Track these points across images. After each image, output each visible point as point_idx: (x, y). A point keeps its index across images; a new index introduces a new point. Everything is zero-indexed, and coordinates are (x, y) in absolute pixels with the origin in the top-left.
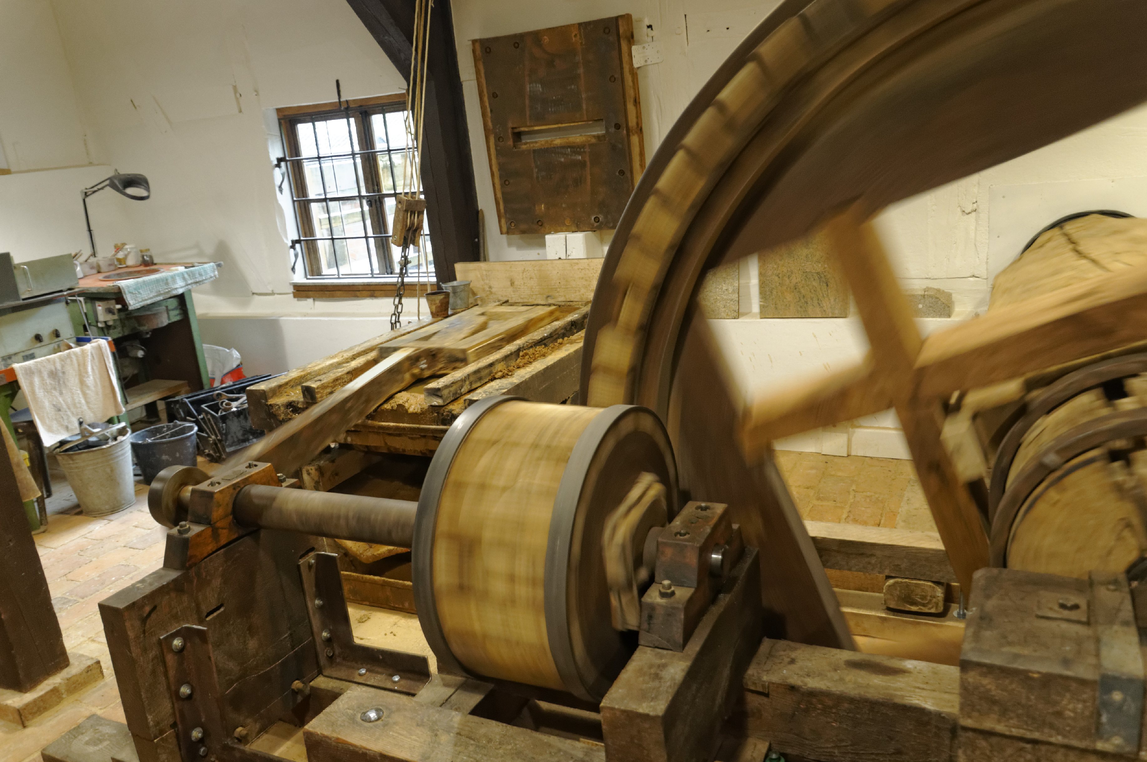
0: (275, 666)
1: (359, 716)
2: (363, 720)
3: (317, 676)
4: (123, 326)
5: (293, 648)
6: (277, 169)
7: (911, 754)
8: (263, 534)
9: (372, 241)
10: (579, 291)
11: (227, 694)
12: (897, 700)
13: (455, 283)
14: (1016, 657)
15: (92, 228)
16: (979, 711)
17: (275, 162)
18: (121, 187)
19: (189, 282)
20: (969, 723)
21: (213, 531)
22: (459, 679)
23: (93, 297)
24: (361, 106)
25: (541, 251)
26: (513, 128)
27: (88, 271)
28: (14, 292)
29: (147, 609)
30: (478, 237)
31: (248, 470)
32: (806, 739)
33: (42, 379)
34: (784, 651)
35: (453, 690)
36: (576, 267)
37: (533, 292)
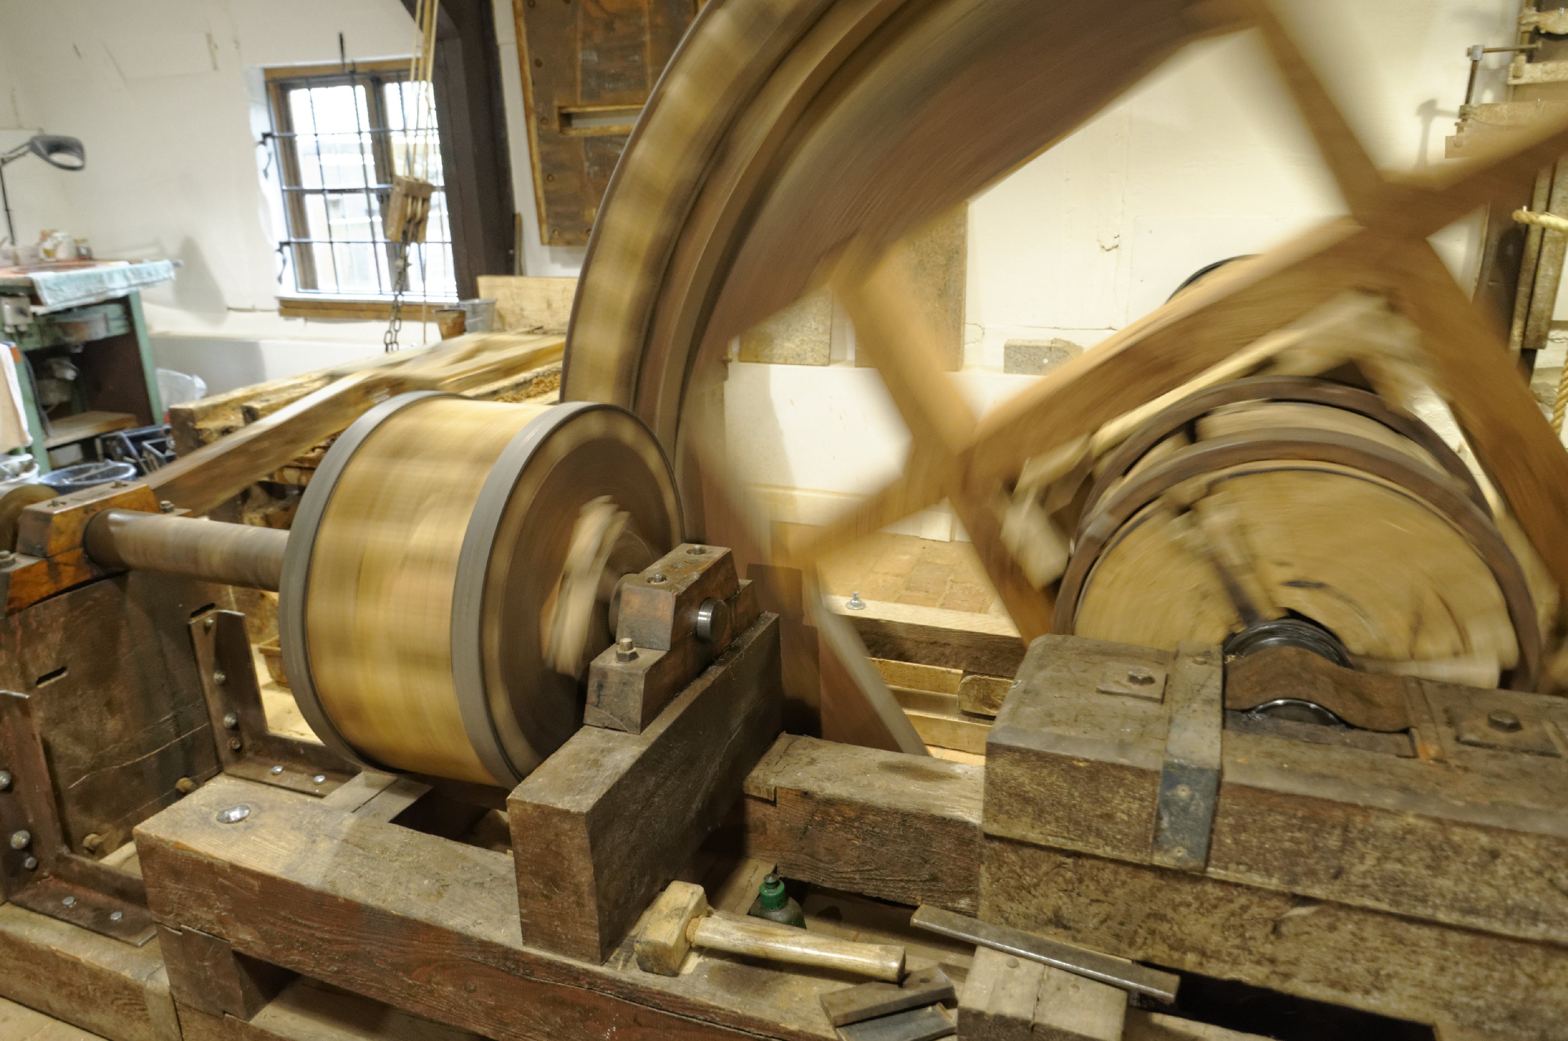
0: (149, 757)
1: (216, 814)
2: (219, 820)
3: (216, 775)
4: (42, 333)
5: (178, 735)
6: (262, 147)
7: (950, 880)
8: (132, 578)
9: (382, 249)
11: (72, 789)
12: (937, 812)
13: (477, 301)
14: (1060, 738)
15: (11, 206)
16: (1007, 812)
17: (260, 138)
18: (44, 151)
19: (134, 282)
20: (994, 829)
21: (49, 566)
22: (387, 778)
24: (372, 71)
26: (560, 108)
30: (512, 246)
31: (113, 490)
32: (821, 861)
34: (804, 749)
35: (376, 791)
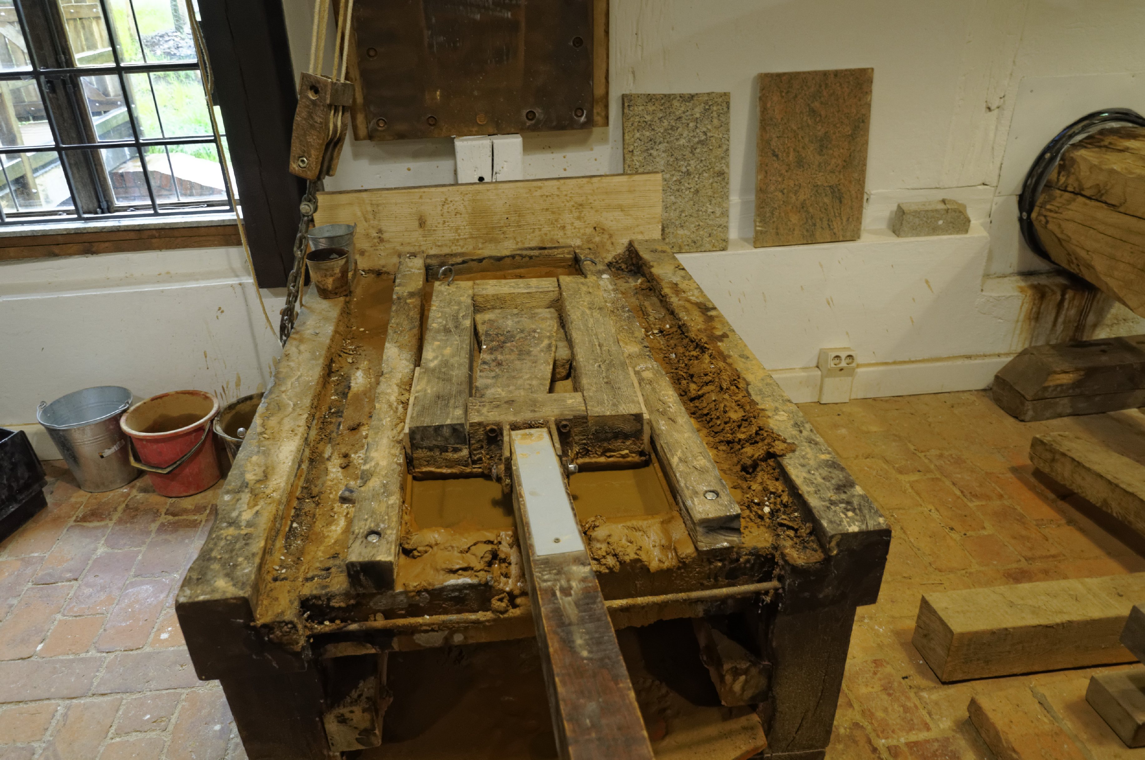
10: (540, 230)
25: (444, 165)
36: (538, 193)
37: (459, 235)
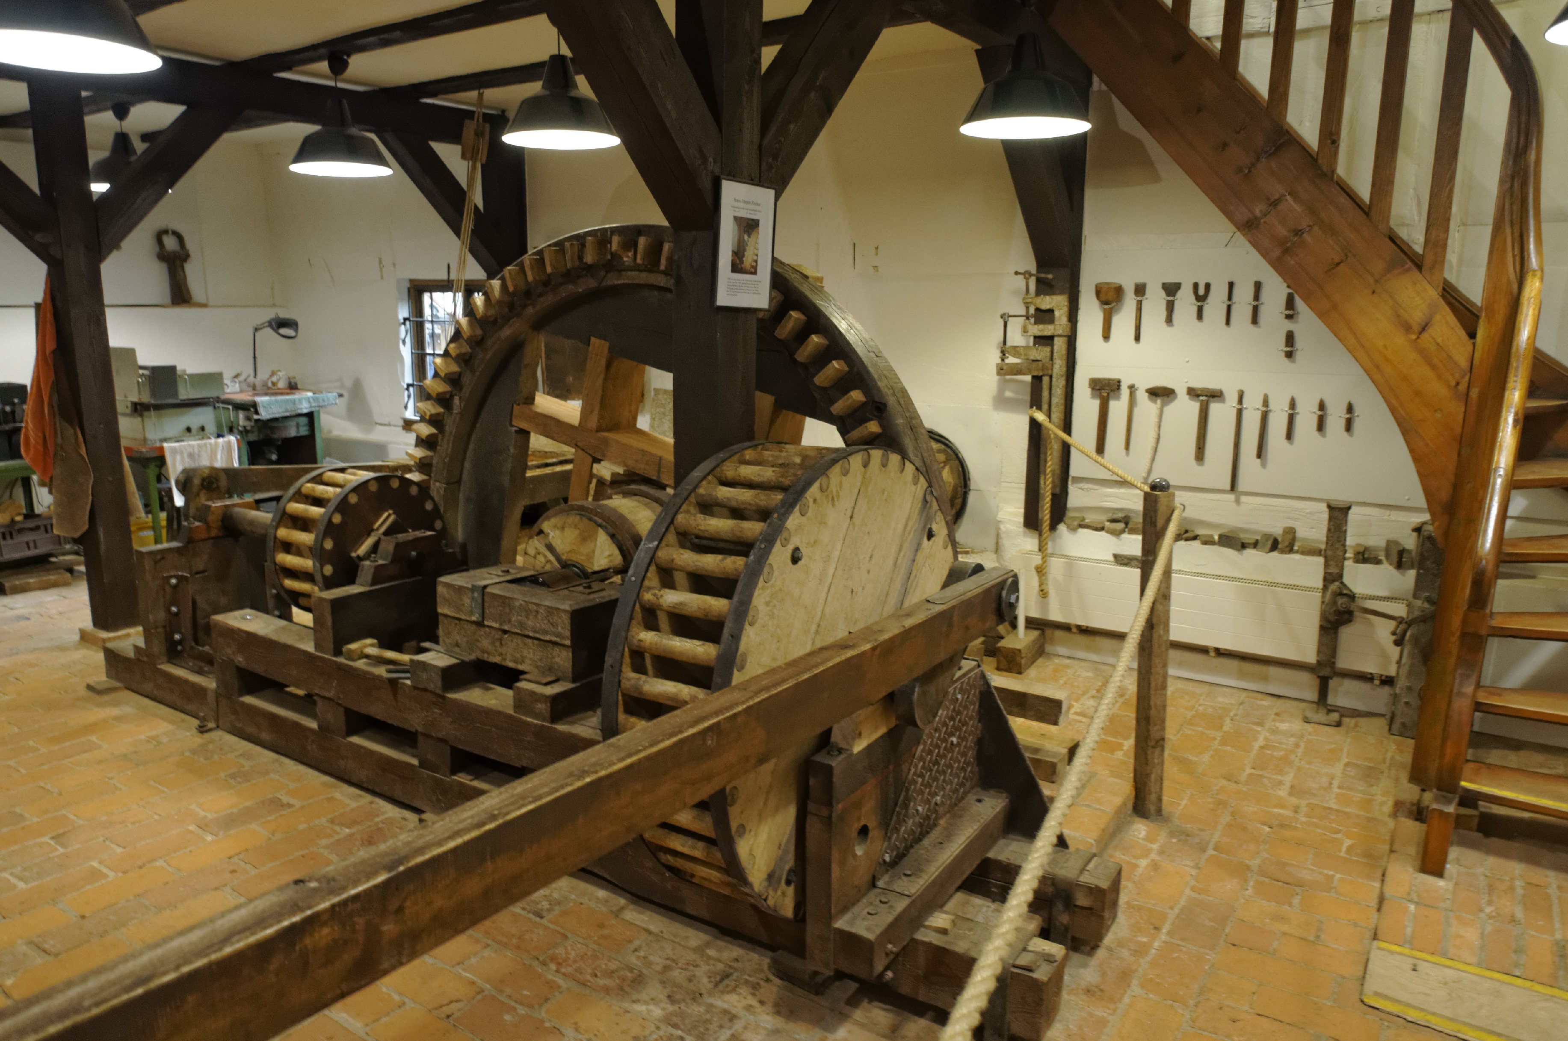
4: (260, 431)
17: (402, 321)
19: (314, 405)
23: (239, 407)
27: (244, 386)
28: (175, 394)
29: (159, 557)
33: (182, 457)
